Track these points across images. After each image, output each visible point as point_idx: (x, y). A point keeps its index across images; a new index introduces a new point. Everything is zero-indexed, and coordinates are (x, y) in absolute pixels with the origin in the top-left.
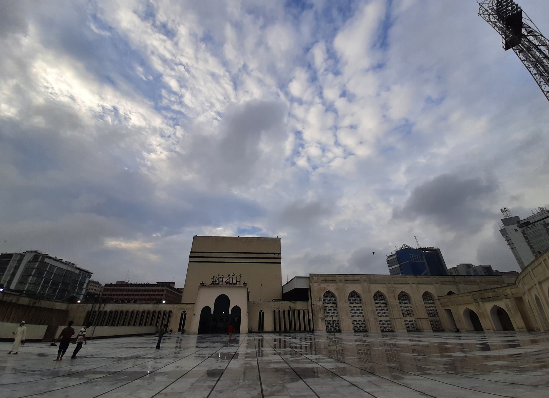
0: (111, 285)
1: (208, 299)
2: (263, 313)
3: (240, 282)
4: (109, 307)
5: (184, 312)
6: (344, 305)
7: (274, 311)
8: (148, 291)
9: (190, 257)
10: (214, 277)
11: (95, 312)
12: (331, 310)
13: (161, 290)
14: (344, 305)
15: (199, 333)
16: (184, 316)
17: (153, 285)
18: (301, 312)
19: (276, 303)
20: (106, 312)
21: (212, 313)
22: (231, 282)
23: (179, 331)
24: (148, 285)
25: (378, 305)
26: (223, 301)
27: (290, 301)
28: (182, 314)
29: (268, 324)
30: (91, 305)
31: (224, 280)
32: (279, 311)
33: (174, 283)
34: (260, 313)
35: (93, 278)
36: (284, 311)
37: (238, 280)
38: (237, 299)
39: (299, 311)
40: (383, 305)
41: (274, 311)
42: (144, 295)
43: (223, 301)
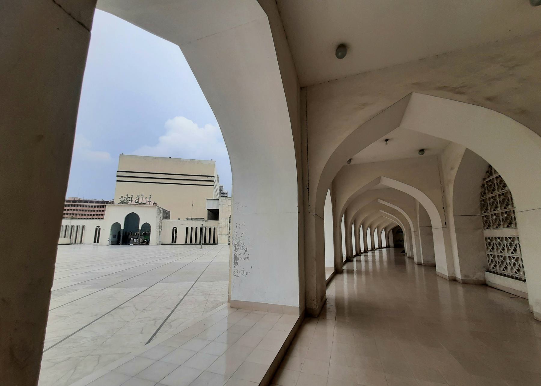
1: (116, 216)
2: (176, 229)
3: (150, 202)
5: (98, 227)
10: (122, 197)
16: (98, 230)
21: (122, 228)
23: (95, 242)
26: (132, 219)
28: (96, 229)
29: (181, 237)
38: (147, 216)
39: (210, 228)
41: (187, 228)
43: (132, 219)
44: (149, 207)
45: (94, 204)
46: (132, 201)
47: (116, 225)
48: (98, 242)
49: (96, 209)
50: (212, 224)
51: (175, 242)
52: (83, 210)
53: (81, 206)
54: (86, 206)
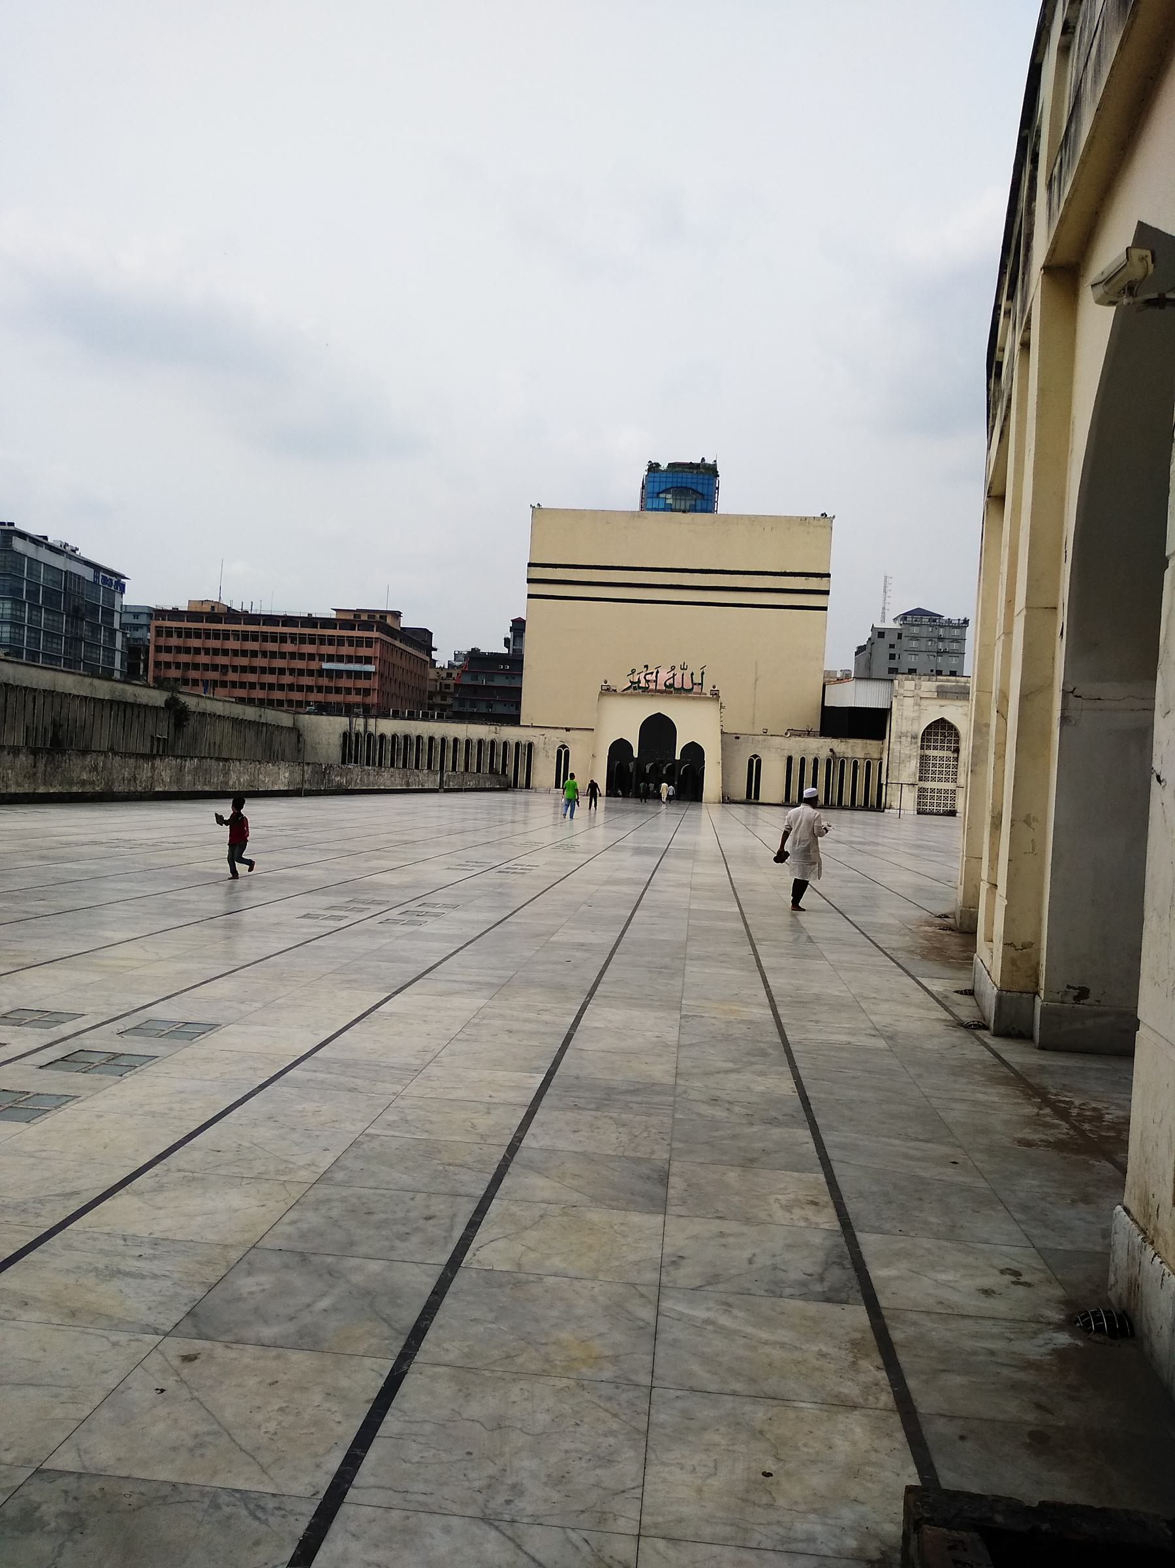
0: (175, 614)
3: (701, 684)
4: (387, 727)
7: (790, 759)
8: (312, 642)
9: (529, 581)
10: (633, 672)
11: (357, 735)
12: (941, 766)
13: (359, 642)
15: (607, 795)
17: (326, 623)
18: (862, 765)
19: (793, 738)
20: (382, 736)
21: (636, 755)
24: (310, 621)
26: (658, 730)
27: (834, 736)
30: (346, 720)
31: (661, 681)
32: (803, 760)
33: (397, 615)
34: (751, 762)
35: (134, 596)
36: (816, 761)
37: (697, 680)
38: (694, 725)
39: (855, 763)
42: (302, 656)
43: (658, 730)
44: (701, 697)
45: (280, 629)
46: (656, 681)
47: (619, 748)
49: (289, 647)
50: (853, 749)
51: (757, 797)
52: (244, 653)
54: (255, 639)
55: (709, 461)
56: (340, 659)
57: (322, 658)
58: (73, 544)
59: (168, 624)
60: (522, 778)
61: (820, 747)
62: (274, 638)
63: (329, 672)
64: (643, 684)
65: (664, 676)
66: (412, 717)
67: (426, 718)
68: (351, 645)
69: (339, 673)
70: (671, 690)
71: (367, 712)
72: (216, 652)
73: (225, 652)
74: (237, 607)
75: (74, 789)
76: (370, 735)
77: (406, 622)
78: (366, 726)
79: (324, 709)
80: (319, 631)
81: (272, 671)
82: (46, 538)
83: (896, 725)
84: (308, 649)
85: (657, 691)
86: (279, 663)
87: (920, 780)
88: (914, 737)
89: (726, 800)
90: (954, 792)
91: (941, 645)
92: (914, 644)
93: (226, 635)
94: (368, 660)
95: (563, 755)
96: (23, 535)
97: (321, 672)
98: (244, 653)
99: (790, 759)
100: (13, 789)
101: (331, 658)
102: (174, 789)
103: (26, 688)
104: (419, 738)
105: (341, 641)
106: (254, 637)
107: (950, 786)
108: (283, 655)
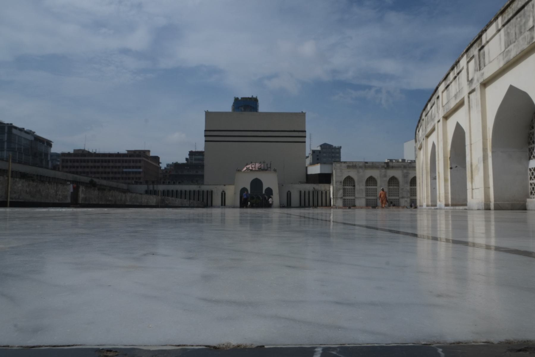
0: (69, 154)
1: (245, 181)
3: (270, 168)
6: (360, 187)
7: (300, 192)
9: (205, 136)
13: (136, 161)
14: (360, 187)
21: (249, 192)
22: (262, 168)
23: (222, 205)
24: (118, 155)
25: (391, 187)
26: (257, 184)
28: (222, 194)
32: (305, 192)
33: (149, 151)
34: (288, 193)
35: (55, 149)
37: (269, 166)
40: (395, 187)
42: (116, 167)
43: (257, 184)
48: (225, 205)
49: (111, 164)
51: (290, 205)
52: (95, 167)
53: (92, 162)
55: (255, 96)
56: (130, 167)
57: (123, 167)
58: (33, 130)
59: (66, 158)
60: (209, 203)
61: (310, 187)
62: (106, 161)
63: (126, 172)
64: (250, 168)
65: (258, 165)
66: (169, 183)
67: (174, 183)
68: (133, 162)
69: (129, 173)
70: (260, 169)
71: (153, 183)
72: (84, 167)
73: (88, 167)
74: (91, 151)
75: (108, 203)
76: (155, 191)
77: (152, 154)
78: (153, 187)
79: (136, 183)
80: (121, 158)
81: (105, 173)
82: (24, 129)
83: (334, 178)
84: (118, 164)
85: (255, 171)
86: (108, 170)
87: (344, 196)
88: (341, 182)
89: (282, 206)
90: (354, 199)
91: (333, 155)
92: (325, 155)
93: (88, 161)
94: (140, 167)
95: (223, 194)
96: (16, 128)
97: (123, 173)
98: (95, 167)
99: (300, 192)
100: (94, 203)
101: (126, 167)
102: (130, 204)
103: (47, 177)
104: (172, 191)
105: (130, 161)
106: (98, 161)
107: (353, 198)
108: (109, 167)
